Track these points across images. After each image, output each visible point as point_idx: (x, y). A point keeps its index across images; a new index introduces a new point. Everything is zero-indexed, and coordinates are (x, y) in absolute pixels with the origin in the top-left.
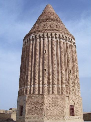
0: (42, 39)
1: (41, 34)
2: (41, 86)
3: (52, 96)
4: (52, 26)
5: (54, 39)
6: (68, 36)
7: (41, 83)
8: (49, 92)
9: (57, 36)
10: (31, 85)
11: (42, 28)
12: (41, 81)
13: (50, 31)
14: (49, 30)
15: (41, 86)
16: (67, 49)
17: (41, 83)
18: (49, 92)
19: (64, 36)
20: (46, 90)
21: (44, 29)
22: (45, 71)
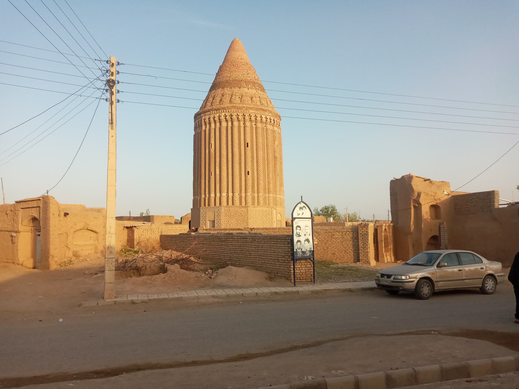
0: (242, 123)
1: (241, 114)
2: (243, 195)
3: (258, 208)
4: (254, 99)
5: (259, 125)
6: (275, 119)
7: (243, 191)
8: (253, 204)
9: (264, 119)
10: (228, 192)
11: (239, 102)
12: (243, 188)
13: (254, 111)
14: (251, 108)
15: (243, 195)
16: (274, 140)
17: (243, 191)
18: (253, 204)
19: (272, 118)
20: (250, 200)
21: (244, 105)
22: (248, 174)
